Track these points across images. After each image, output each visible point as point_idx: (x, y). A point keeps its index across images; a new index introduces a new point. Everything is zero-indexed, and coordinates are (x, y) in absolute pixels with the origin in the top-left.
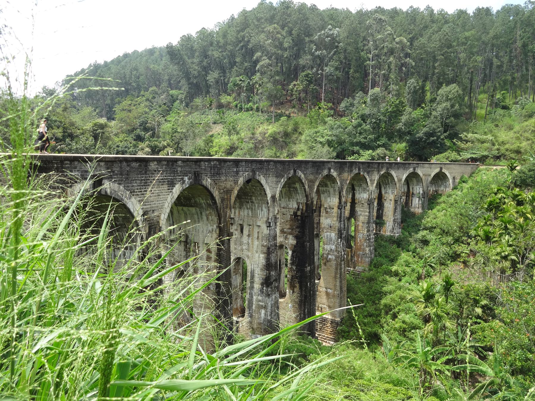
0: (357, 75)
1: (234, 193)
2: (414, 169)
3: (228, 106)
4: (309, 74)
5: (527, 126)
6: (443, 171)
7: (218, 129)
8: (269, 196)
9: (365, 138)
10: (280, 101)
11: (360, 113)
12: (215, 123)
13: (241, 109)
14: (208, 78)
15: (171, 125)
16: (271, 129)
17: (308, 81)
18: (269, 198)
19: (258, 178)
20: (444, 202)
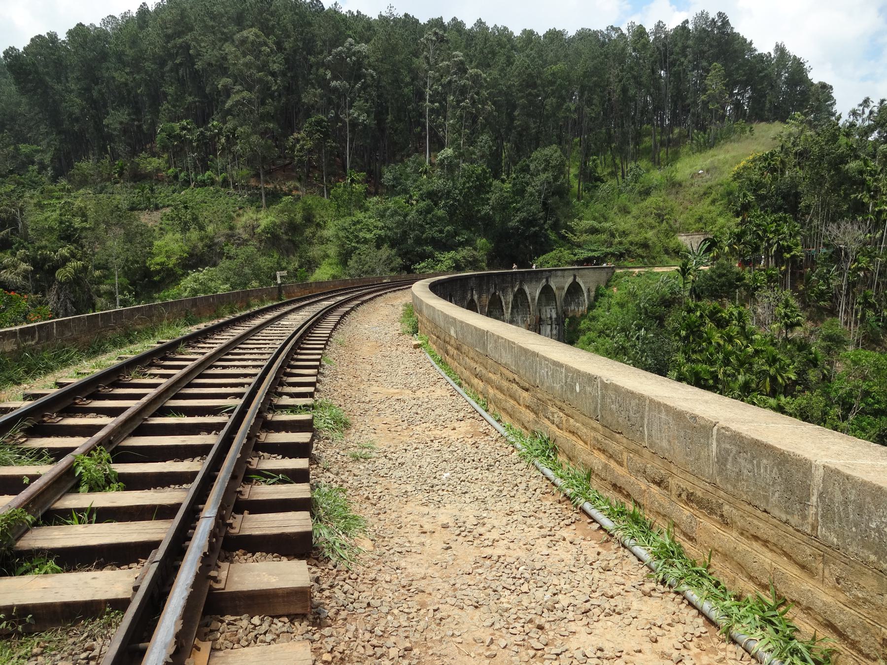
0: (401, 126)
2: (547, 281)
3: (154, 177)
4: (323, 120)
5: (647, 208)
6: (578, 280)
7: (148, 219)
9: (441, 232)
10: (271, 170)
11: (425, 189)
12: (132, 209)
13: (187, 183)
14: (105, 122)
15: (55, 215)
16: (268, 219)
17: (321, 132)
20: (589, 329)
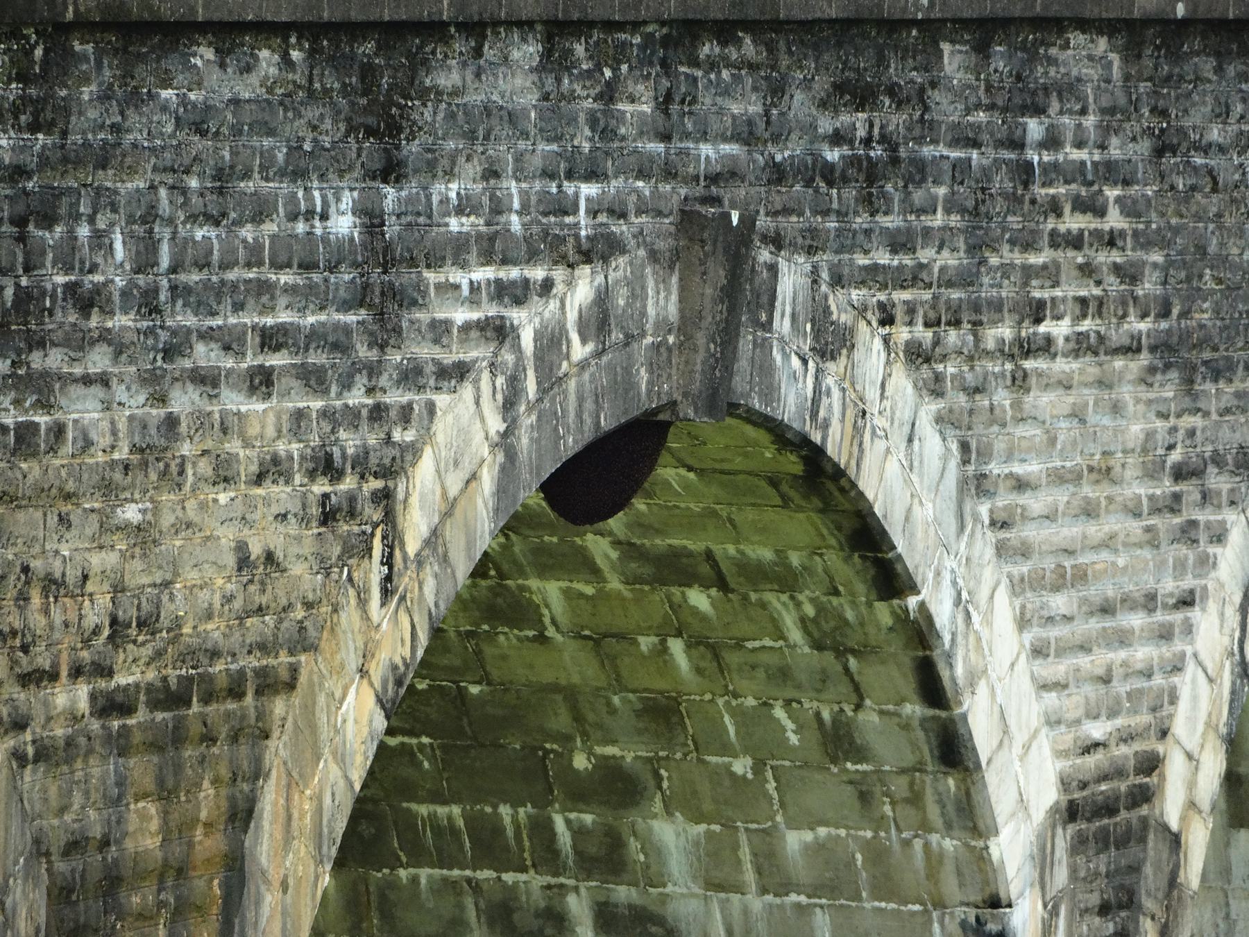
1: (309, 745)
8: (1023, 783)
18: (1012, 848)
19: (793, 389)
